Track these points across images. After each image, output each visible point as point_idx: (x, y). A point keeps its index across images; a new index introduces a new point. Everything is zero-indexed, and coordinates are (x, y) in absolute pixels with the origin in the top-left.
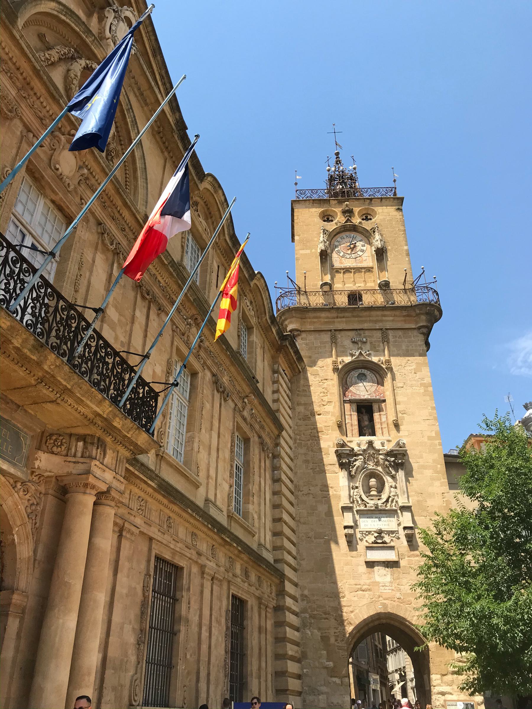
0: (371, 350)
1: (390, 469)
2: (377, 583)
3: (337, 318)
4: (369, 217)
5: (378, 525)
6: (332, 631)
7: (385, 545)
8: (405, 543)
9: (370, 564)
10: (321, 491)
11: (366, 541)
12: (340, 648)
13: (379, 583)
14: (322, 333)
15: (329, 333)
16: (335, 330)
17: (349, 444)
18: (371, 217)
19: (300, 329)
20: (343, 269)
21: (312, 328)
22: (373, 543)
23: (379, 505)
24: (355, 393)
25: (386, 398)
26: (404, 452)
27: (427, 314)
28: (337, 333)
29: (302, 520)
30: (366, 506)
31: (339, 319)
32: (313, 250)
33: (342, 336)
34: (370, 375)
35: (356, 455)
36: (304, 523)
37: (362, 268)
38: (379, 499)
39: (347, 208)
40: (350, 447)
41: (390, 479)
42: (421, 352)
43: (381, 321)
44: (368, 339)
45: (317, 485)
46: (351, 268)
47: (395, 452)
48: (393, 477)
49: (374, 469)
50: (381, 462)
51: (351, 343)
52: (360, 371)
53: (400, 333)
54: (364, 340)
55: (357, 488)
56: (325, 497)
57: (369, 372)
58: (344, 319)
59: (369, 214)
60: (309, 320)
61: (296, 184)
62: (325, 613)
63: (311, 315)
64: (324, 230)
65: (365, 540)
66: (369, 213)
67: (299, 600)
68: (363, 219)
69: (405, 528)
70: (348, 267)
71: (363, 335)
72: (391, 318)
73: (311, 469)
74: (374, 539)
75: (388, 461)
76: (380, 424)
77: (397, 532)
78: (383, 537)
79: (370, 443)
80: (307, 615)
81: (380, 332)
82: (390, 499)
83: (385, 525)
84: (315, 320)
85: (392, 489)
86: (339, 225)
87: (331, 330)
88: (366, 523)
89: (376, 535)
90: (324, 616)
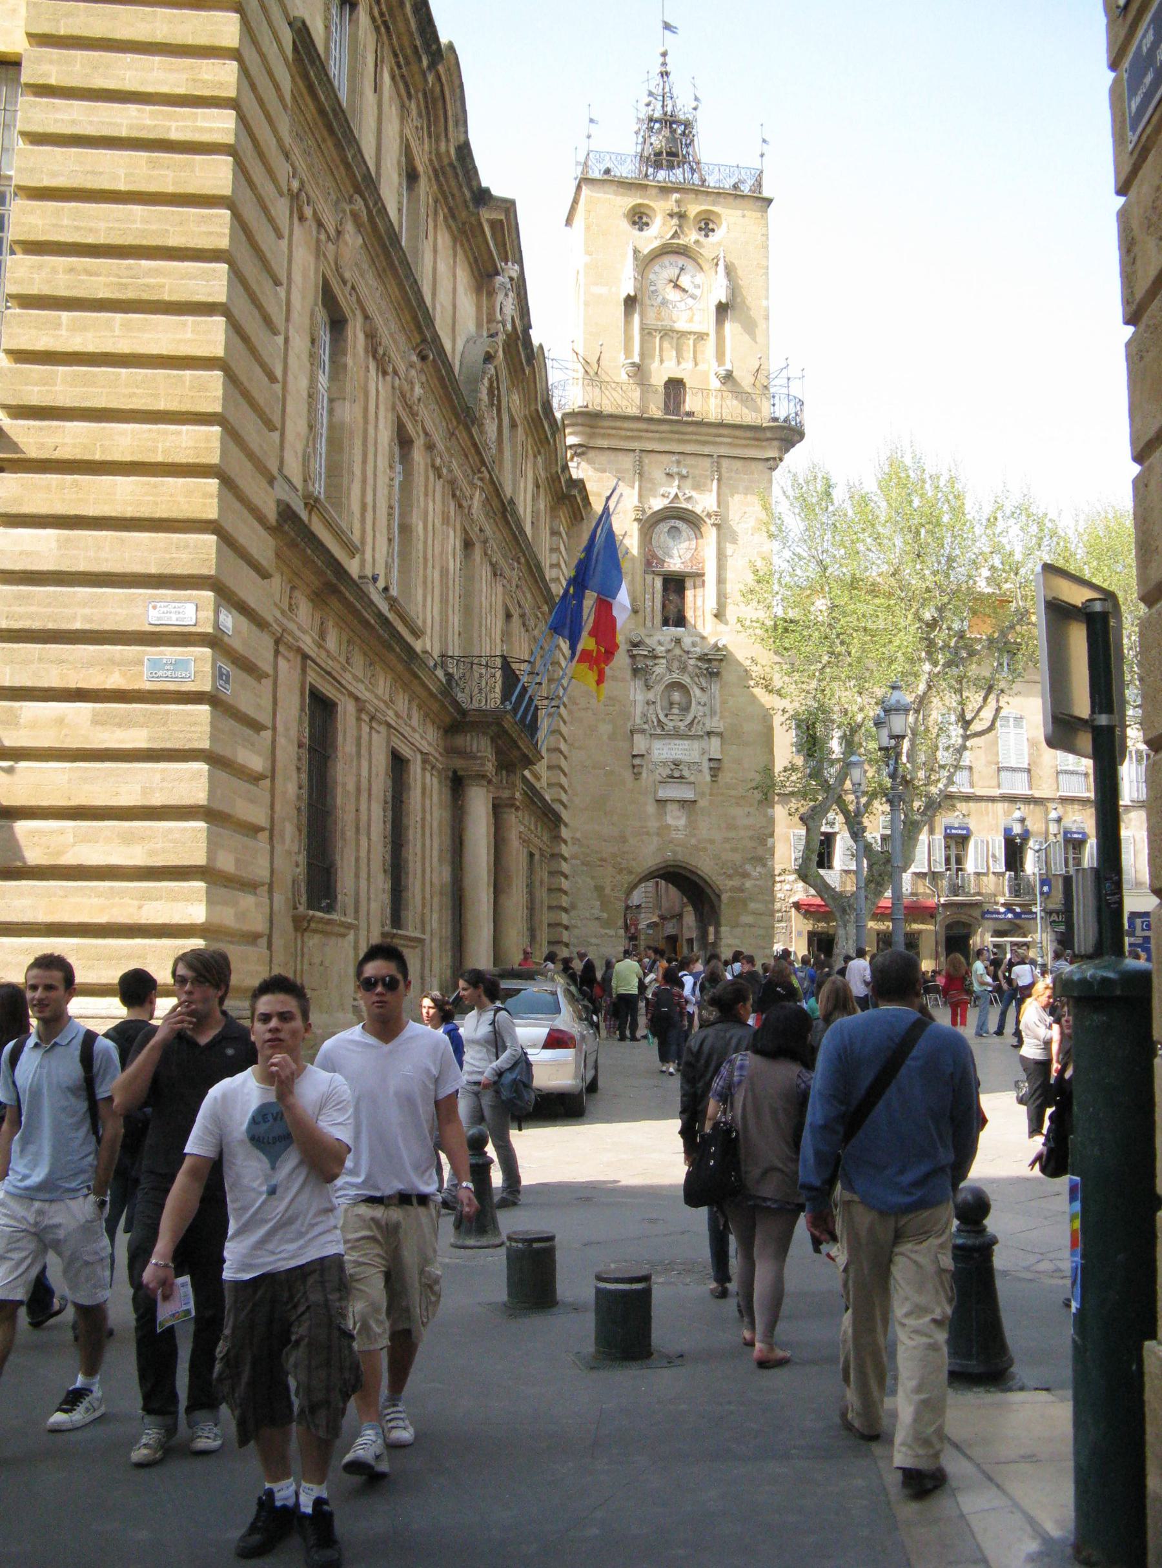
2: (668, 827)
4: (711, 226)
8: (708, 778)
9: (661, 803)
12: (617, 898)
13: (670, 826)
15: (632, 454)
16: (642, 451)
17: (647, 641)
18: (715, 227)
21: (605, 443)
22: (668, 777)
25: (706, 571)
27: (782, 440)
28: (644, 455)
30: (663, 729)
35: (656, 657)
37: (690, 333)
39: (676, 210)
50: (690, 668)
52: (673, 523)
54: (684, 472)
57: (685, 526)
58: (657, 435)
60: (602, 431)
61: (589, 137)
63: (606, 423)
64: (636, 251)
67: (569, 843)
68: (700, 229)
69: (710, 760)
72: (729, 440)
79: (678, 641)
80: (578, 862)
84: (614, 432)
85: (700, 707)
87: (634, 451)
90: (599, 863)
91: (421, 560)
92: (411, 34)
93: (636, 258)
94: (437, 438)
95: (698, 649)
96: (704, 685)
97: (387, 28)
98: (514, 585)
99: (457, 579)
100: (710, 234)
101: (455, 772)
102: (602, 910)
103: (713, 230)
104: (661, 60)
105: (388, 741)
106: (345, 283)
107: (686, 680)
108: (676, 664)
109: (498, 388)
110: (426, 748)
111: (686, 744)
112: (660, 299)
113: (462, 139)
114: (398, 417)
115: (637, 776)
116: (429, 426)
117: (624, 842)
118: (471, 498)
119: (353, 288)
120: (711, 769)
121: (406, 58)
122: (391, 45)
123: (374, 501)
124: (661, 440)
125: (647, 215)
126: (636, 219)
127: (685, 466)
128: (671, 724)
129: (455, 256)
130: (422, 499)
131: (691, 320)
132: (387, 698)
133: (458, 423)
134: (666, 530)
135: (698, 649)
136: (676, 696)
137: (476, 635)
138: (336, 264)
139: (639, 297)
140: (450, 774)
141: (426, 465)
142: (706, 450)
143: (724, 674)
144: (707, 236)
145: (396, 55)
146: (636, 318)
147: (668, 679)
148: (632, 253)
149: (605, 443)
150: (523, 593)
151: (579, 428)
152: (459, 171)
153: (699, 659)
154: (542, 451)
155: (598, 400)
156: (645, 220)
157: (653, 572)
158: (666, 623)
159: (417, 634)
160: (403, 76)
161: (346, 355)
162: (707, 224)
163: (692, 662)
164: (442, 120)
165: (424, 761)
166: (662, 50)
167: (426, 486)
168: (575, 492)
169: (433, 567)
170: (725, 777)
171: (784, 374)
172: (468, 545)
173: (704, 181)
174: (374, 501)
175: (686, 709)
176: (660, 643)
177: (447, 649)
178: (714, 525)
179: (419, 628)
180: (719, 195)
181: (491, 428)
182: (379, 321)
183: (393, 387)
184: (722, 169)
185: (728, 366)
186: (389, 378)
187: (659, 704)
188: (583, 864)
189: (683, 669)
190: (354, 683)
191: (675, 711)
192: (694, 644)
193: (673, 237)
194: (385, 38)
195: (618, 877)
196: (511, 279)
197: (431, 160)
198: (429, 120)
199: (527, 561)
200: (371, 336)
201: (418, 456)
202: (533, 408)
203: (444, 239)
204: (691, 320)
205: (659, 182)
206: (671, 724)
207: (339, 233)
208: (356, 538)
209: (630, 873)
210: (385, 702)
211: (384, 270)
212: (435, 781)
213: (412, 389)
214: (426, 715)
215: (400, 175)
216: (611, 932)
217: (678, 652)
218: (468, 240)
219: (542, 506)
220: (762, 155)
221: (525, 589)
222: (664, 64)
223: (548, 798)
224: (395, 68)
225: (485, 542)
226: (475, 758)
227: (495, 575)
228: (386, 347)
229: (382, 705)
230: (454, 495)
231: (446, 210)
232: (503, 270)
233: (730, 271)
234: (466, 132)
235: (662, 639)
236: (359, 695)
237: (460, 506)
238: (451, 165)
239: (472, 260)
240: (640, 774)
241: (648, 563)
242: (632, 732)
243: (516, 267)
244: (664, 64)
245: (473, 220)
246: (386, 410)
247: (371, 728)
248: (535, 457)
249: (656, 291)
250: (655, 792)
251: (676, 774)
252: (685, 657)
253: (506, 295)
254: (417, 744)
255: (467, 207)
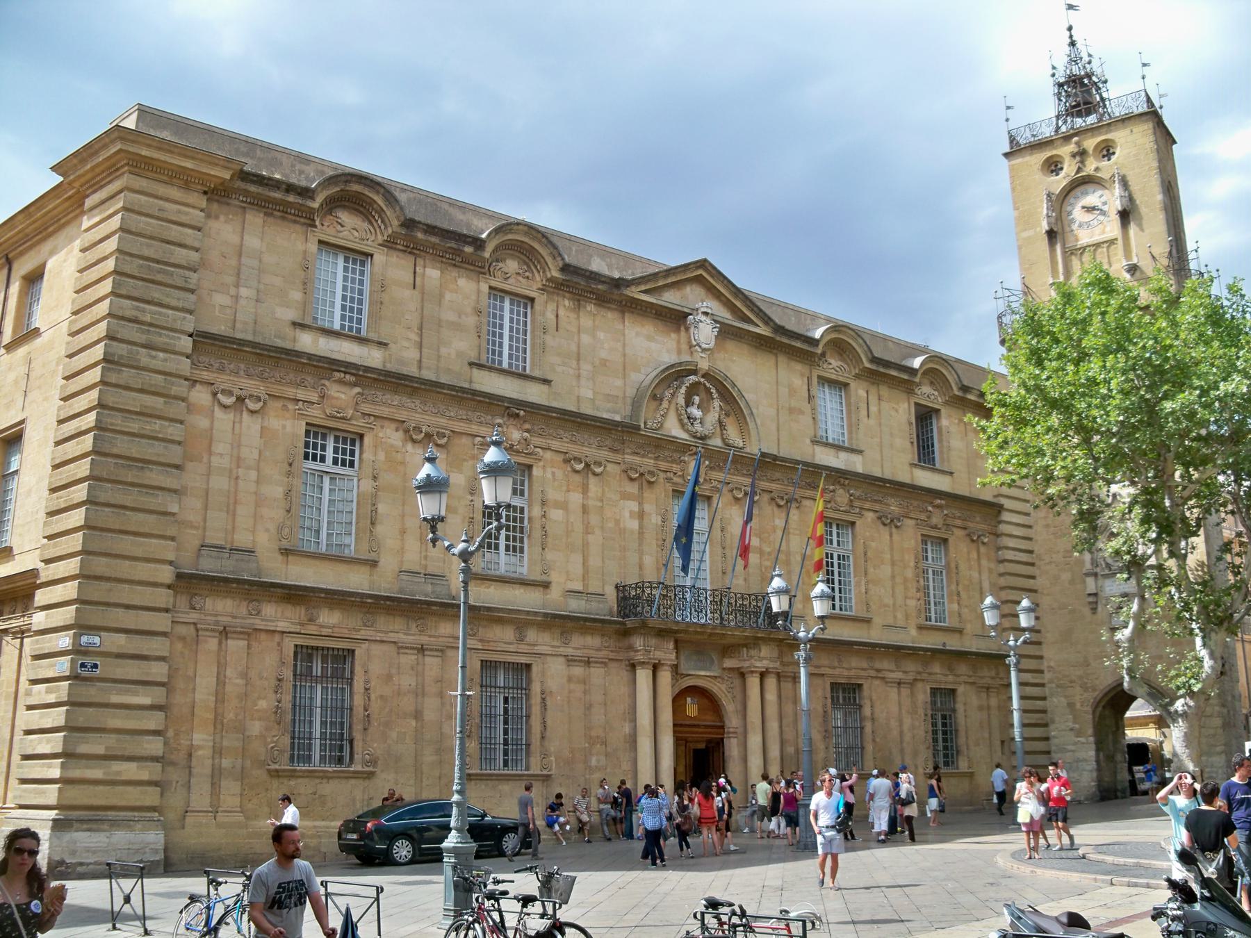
4: (1111, 151)
6: (1077, 698)
12: (1086, 712)
29: (1045, 592)
36: (1048, 595)
37: (1103, 243)
39: (1076, 150)
62: (1071, 682)
64: (1048, 195)
68: (1104, 156)
80: (1054, 685)
86: (1069, 179)
102: (1075, 722)
117: (1088, 665)
131: (1103, 232)
146: (1058, 248)
162: (1108, 150)
188: (1058, 686)
193: (1078, 172)
195: (1086, 695)
209: (1094, 690)
216: (1082, 740)
233: (1125, 183)
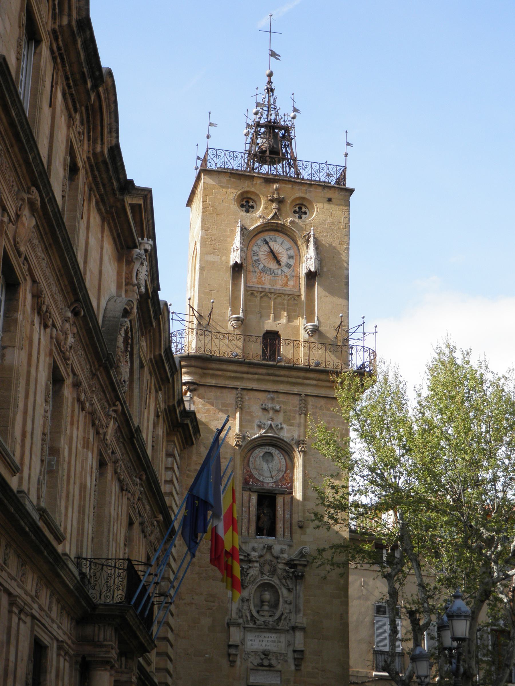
0: (284, 423)
1: (288, 581)
3: (248, 373)
4: (304, 210)
5: (266, 645)
7: (272, 669)
8: (293, 668)
10: (206, 601)
11: (251, 662)
14: (226, 391)
15: (235, 391)
18: (307, 211)
19: (198, 382)
20: (261, 292)
21: (213, 382)
22: (258, 665)
23: (271, 623)
24: (257, 479)
26: (305, 563)
28: (244, 392)
30: (255, 623)
31: (250, 376)
32: (224, 258)
33: (250, 399)
34: (279, 456)
35: (250, 561)
38: (270, 616)
39: (276, 196)
40: (246, 552)
41: (285, 592)
42: (344, 432)
43: (302, 384)
44: (282, 406)
45: (201, 594)
46: (271, 293)
47: (295, 562)
48: (289, 590)
49: (269, 580)
50: (279, 571)
51: (261, 410)
52: (267, 449)
53: (322, 402)
54: (278, 408)
55: (248, 600)
56: (209, 609)
57: (277, 452)
58: (256, 376)
59: (305, 206)
60: (211, 372)
61: (208, 137)
63: (214, 366)
65: (250, 660)
66: (304, 203)
68: (295, 212)
69: (295, 651)
70: (267, 290)
71: (276, 399)
72: (314, 382)
73: (197, 573)
74: (260, 661)
75: (287, 572)
76: (282, 522)
77: (284, 655)
78: (269, 660)
79: (269, 548)
81: (298, 398)
82: (283, 617)
83: (273, 646)
85: (287, 606)
87: (237, 389)
88: (253, 643)
89: (263, 656)
91: (65, 477)
92: (80, 64)
93: (242, 234)
94: (82, 377)
95: (285, 556)
96: (291, 586)
97: (62, 59)
98: (136, 499)
99: (93, 493)
100: (303, 216)
101: (84, 658)
103: (305, 213)
104: (267, 79)
105: (32, 630)
106: (20, 254)
107: (275, 581)
108: (267, 568)
109: (132, 339)
110: (62, 637)
111: (274, 636)
112: (261, 266)
113: (114, 142)
114: (54, 361)
115: (232, 663)
116: (78, 370)
118: (107, 427)
119: (26, 259)
120: (295, 659)
121: (74, 81)
122: (64, 70)
123: (33, 428)
124: (258, 380)
125: (254, 201)
126: (244, 203)
127: (278, 402)
128: (263, 619)
129: (103, 232)
130: (69, 427)
132: (33, 593)
133: (100, 366)
134: (262, 454)
135: (285, 556)
136: (267, 596)
137: (105, 540)
138: (15, 240)
139: (244, 265)
140: (80, 659)
141: (73, 399)
142: (296, 390)
143: (307, 576)
144: (300, 217)
145: (67, 79)
147: (260, 580)
148: (239, 229)
149: (213, 382)
150: (143, 505)
151: (192, 369)
152: (110, 167)
153: (287, 564)
154: (163, 387)
155: (208, 347)
156: (251, 203)
157: (250, 490)
158: (260, 531)
159: (60, 539)
160: (71, 95)
161: (18, 312)
162: (300, 208)
163: (281, 566)
164: (99, 128)
165: (59, 648)
166: (268, 72)
167: (72, 417)
168: (188, 422)
169: (75, 483)
170: (307, 667)
171: (361, 329)
172: (102, 464)
173: (298, 174)
174: (33, 428)
175: (275, 606)
176: (254, 549)
177: (81, 553)
178: (301, 451)
179: (61, 534)
180: (312, 184)
181: (125, 370)
182: (43, 285)
183: (52, 337)
184: (313, 165)
185: (316, 323)
186: (48, 330)
187: (251, 602)
189: (273, 572)
190: (9, 580)
191: (266, 608)
192: (282, 551)
193: (273, 218)
194: (60, 66)
196: (146, 251)
197: (88, 158)
198: (89, 127)
199: (147, 478)
200: (37, 296)
201: (68, 392)
202: (157, 353)
203: (95, 219)
204: (286, 285)
205: (262, 174)
206: (263, 619)
207: (18, 216)
208: (17, 459)
210: (32, 597)
211: (50, 245)
212: (67, 665)
213: (66, 339)
214: (63, 608)
215: (65, 169)
217: (268, 557)
218: (114, 220)
219: (160, 432)
220: (346, 155)
221: (144, 501)
222: (270, 82)
223: (156, 680)
224: (66, 88)
225: (115, 462)
226: (101, 646)
227: (122, 489)
228: (48, 306)
229: (28, 599)
230: (93, 425)
231: (98, 196)
232: (140, 244)
234: (117, 137)
235: (256, 545)
236: (12, 590)
237: (98, 433)
238: (105, 162)
239: (115, 235)
240: (235, 662)
241: (246, 482)
242: (228, 625)
243: (151, 242)
244: (270, 82)
245: (118, 204)
246: (46, 354)
247: (20, 619)
248: (157, 392)
249: (258, 260)
250: (247, 679)
251: (266, 663)
252: (275, 561)
253: (142, 264)
254: (55, 634)
255: (115, 195)
